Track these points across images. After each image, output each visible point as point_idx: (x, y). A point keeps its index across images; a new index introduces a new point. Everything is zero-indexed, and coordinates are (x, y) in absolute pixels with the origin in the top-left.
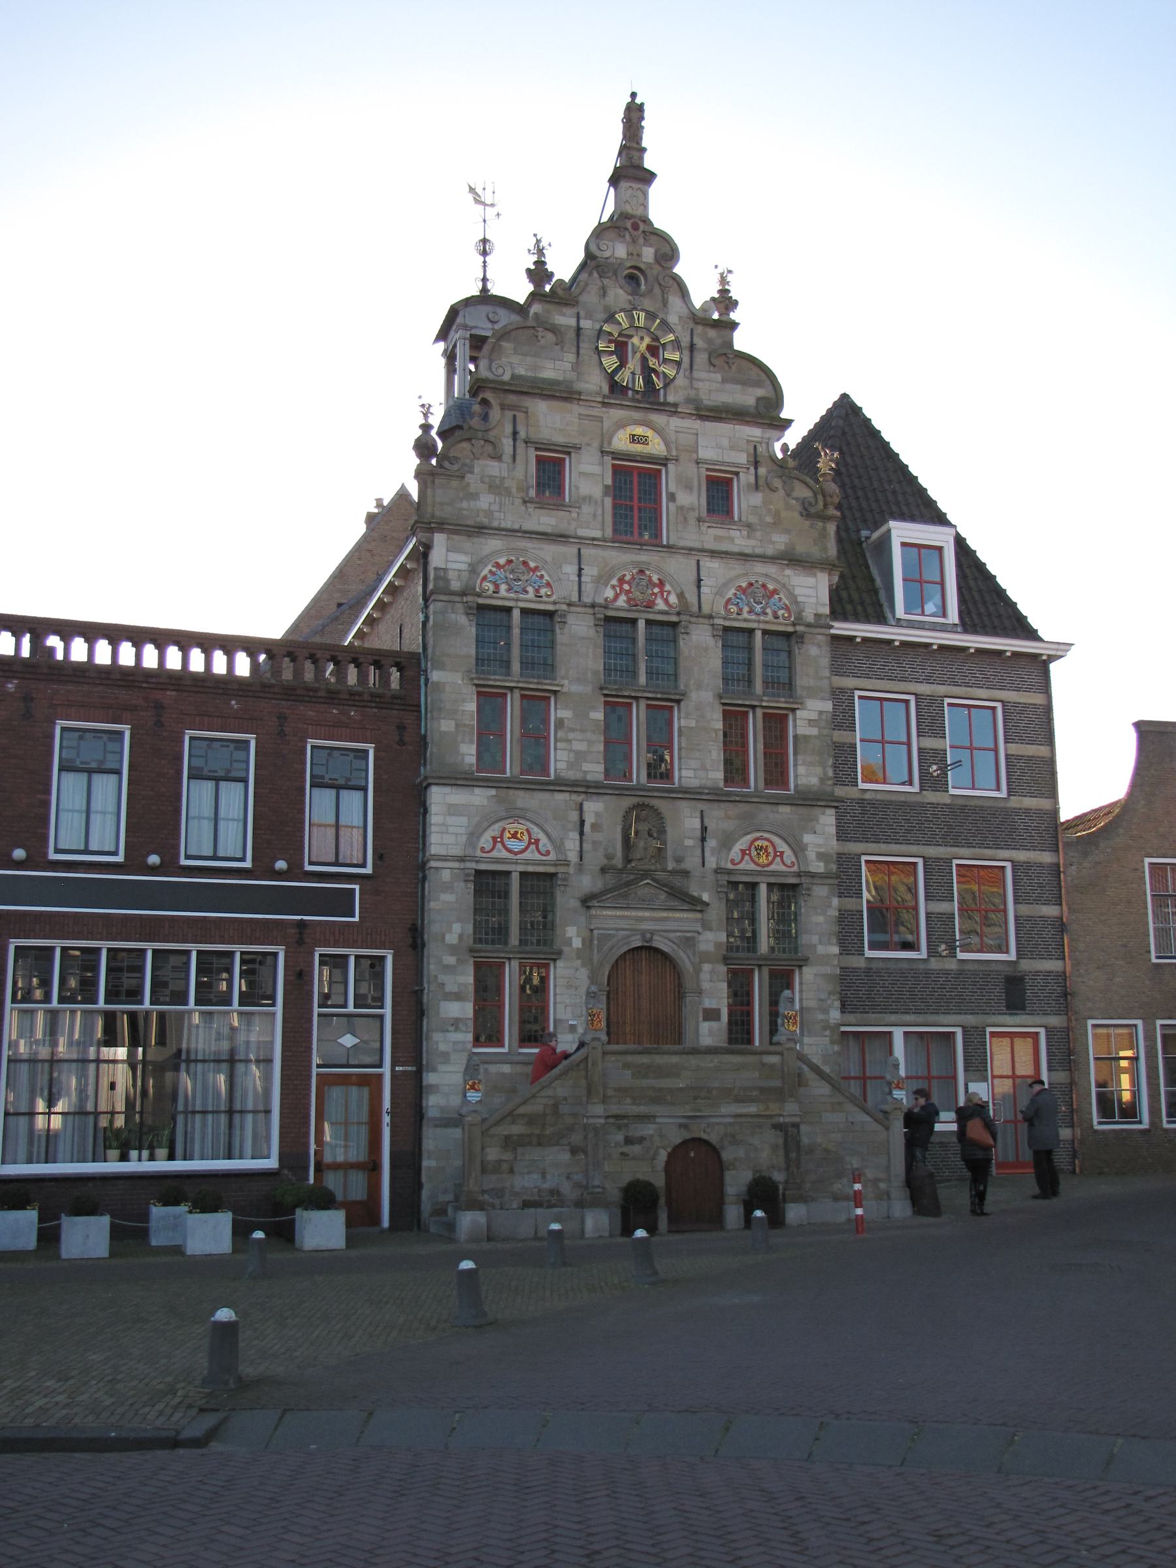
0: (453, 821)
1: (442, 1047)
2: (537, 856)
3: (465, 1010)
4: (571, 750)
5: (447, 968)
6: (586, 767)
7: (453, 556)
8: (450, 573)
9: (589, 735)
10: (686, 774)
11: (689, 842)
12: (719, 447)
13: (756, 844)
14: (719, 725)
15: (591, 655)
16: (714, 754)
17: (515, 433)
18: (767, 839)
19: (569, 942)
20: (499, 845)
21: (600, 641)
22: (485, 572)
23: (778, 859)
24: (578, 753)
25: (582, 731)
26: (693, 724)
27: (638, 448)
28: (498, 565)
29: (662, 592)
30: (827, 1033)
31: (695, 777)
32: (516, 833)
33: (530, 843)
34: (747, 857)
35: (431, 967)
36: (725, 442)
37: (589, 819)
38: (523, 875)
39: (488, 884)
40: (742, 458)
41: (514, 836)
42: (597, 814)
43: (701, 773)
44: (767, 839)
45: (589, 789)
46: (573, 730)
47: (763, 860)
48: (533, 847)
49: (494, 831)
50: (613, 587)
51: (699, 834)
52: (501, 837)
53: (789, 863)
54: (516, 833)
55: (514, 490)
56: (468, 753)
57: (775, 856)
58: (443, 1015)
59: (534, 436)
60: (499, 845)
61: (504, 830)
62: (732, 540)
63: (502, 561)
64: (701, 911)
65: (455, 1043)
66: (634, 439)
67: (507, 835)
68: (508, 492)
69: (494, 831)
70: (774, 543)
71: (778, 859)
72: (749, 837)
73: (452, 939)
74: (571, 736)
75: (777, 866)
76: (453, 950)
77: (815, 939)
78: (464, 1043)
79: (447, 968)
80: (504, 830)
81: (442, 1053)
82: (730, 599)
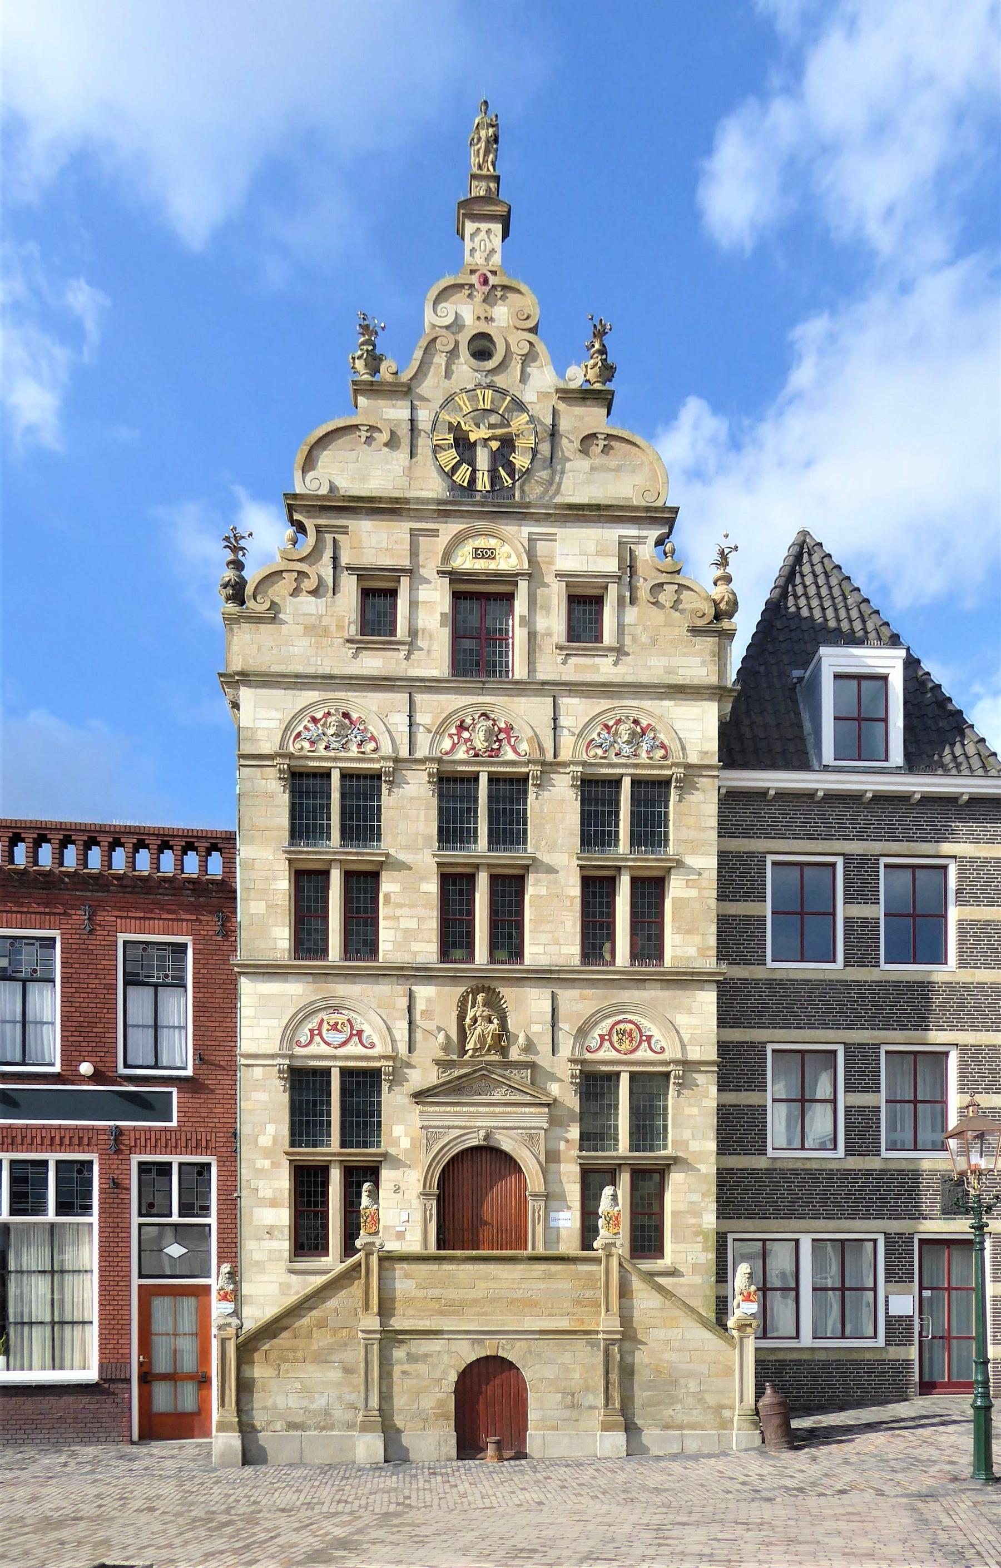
0: (265, 1016)
1: (257, 1256)
2: (360, 1050)
3: (282, 1216)
4: (397, 929)
5: (260, 1173)
6: (416, 947)
7: (262, 713)
8: (259, 732)
9: (421, 911)
10: (535, 951)
11: (536, 1028)
12: (583, 553)
13: (618, 1027)
14: (576, 891)
15: (422, 818)
16: (569, 925)
17: (335, 559)
18: (630, 1022)
19: (396, 1143)
20: (317, 1039)
21: (435, 801)
22: (300, 728)
23: (645, 1045)
24: (406, 931)
25: (412, 906)
26: (544, 892)
27: (480, 565)
28: (314, 720)
29: (509, 738)
30: (700, 1239)
31: (545, 953)
32: (337, 1024)
33: (352, 1035)
34: (607, 1044)
35: (245, 1172)
36: (592, 547)
37: (420, 1006)
38: (345, 1072)
39: (305, 1084)
40: (611, 565)
41: (335, 1027)
42: (429, 1000)
43: (552, 949)
44: (630, 1022)
45: (422, 974)
46: (401, 906)
47: (626, 1046)
48: (356, 1039)
49: (313, 1024)
50: (451, 736)
51: (549, 1017)
52: (320, 1029)
53: (658, 1049)
54: (337, 1024)
55: (333, 628)
56: (280, 938)
57: (641, 1041)
58: (256, 1222)
59: (356, 562)
60: (317, 1039)
61: (322, 1020)
62: (596, 668)
63: (319, 715)
64: (548, 1105)
65: (270, 1251)
66: (479, 554)
67: (325, 1027)
68: (326, 632)
69: (313, 1024)
70: (650, 668)
71: (645, 1045)
72: (610, 1021)
73: (265, 1141)
74: (398, 912)
75: (643, 1054)
76: (267, 1153)
77: (687, 1134)
78: (280, 1251)
79: (260, 1173)
80: (322, 1020)
81: (258, 1262)
82: (593, 740)
